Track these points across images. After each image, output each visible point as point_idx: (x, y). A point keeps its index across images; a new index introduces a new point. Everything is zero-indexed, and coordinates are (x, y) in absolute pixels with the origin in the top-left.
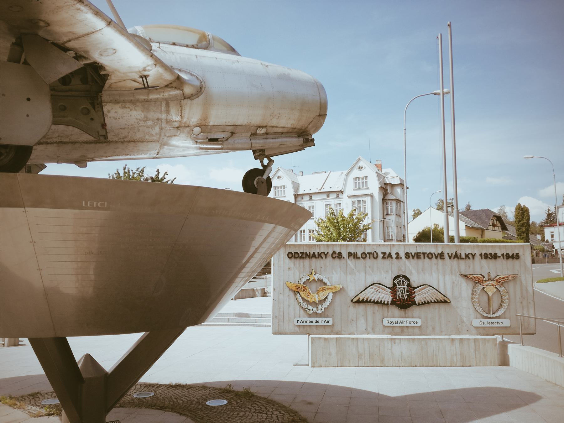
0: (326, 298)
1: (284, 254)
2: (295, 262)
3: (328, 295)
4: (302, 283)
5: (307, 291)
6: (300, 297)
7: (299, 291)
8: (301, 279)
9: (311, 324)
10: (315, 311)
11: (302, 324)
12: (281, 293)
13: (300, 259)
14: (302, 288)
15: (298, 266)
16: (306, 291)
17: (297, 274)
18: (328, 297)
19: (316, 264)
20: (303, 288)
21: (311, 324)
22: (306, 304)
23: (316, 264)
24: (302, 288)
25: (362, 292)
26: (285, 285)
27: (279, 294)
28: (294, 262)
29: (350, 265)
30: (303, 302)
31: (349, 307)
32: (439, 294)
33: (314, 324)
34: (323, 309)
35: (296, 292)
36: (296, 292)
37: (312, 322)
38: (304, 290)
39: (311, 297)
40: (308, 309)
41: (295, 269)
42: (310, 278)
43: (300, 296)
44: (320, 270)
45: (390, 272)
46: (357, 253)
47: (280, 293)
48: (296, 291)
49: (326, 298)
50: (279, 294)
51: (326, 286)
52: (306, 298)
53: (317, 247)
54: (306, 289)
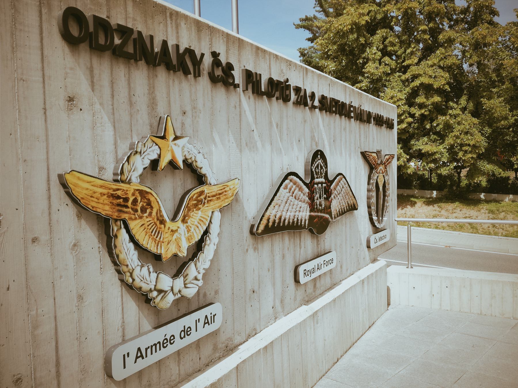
0: (206, 232)
1: (40, 12)
2: (96, 72)
3: (210, 221)
4: (135, 177)
5: (154, 213)
6: (131, 246)
7: (126, 216)
8: (132, 160)
9: (171, 349)
10: (180, 291)
11: (142, 364)
12: (34, 240)
13: (257, 99)
14: (135, 201)
15: (107, 91)
16: (150, 214)
17: (108, 134)
18: (211, 231)
19: (168, 94)
20: (139, 199)
21: (171, 349)
22: (151, 270)
23: (168, 94)
24: (135, 201)
25: (272, 200)
26: (57, 191)
27: (26, 248)
28: (91, 70)
29: (246, 112)
30: (142, 266)
31: (247, 250)
32: (350, 193)
33: (179, 344)
34: (200, 277)
35: (116, 220)
36: (116, 220)
37: (171, 340)
38: (143, 210)
39: (166, 236)
40: (160, 291)
41: (97, 106)
42: (160, 156)
43: (132, 239)
44: (183, 124)
45: (303, 143)
46: (260, 75)
47: (30, 236)
48: (115, 215)
49: (206, 232)
50: (26, 248)
51: (205, 188)
52: (151, 247)
53: (168, 19)
54: (149, 204)
